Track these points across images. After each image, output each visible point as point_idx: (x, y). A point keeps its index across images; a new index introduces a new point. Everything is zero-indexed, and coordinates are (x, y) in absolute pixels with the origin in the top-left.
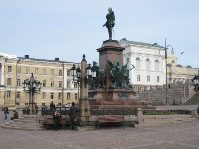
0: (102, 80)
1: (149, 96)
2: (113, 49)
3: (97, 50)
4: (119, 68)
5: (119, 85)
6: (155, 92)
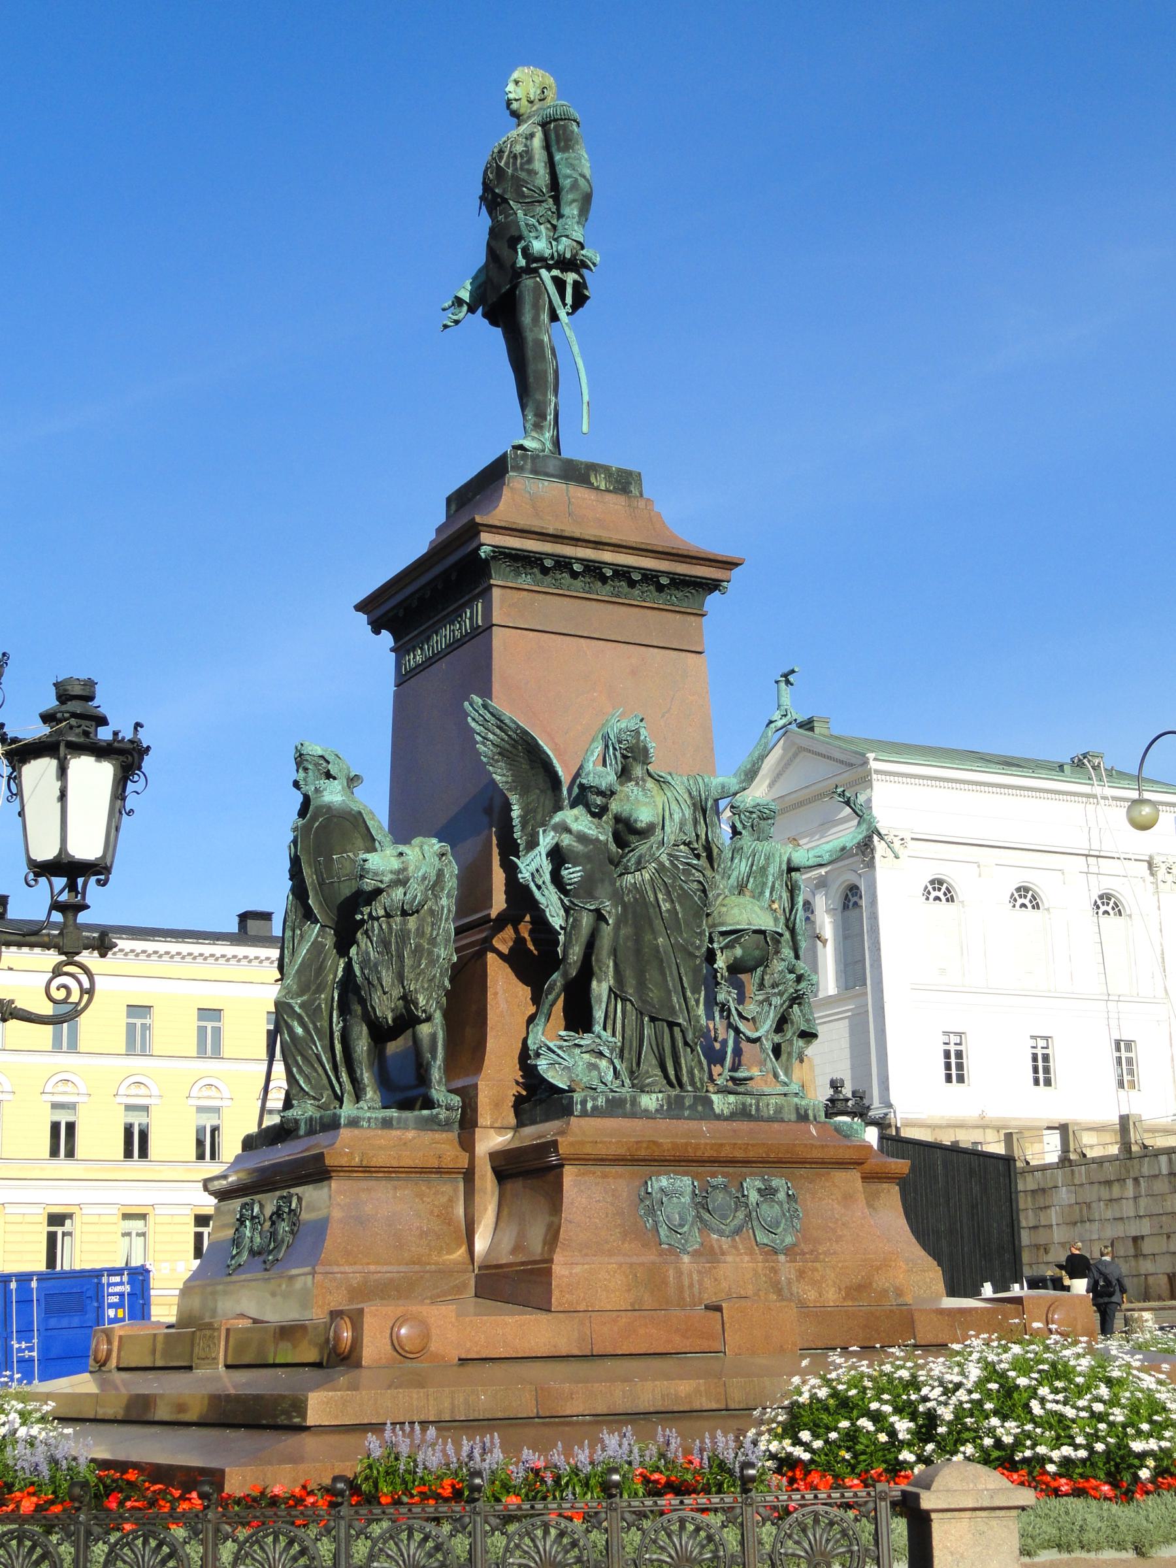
0: (407, 999)
1: (1054, 1216)
2: (563, 564)
3: (359, 607)
4: (644, 816)
5: (649, 1063)
6: (1108, 1183)
